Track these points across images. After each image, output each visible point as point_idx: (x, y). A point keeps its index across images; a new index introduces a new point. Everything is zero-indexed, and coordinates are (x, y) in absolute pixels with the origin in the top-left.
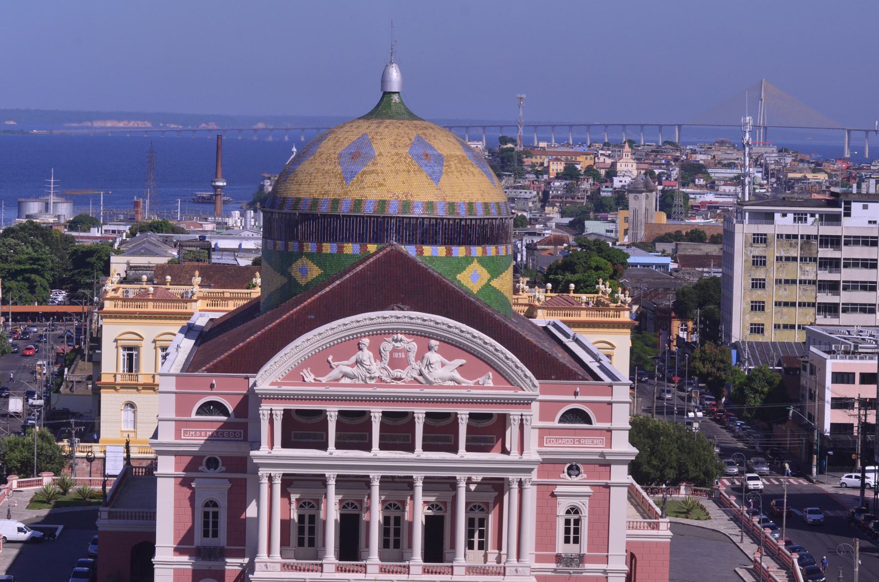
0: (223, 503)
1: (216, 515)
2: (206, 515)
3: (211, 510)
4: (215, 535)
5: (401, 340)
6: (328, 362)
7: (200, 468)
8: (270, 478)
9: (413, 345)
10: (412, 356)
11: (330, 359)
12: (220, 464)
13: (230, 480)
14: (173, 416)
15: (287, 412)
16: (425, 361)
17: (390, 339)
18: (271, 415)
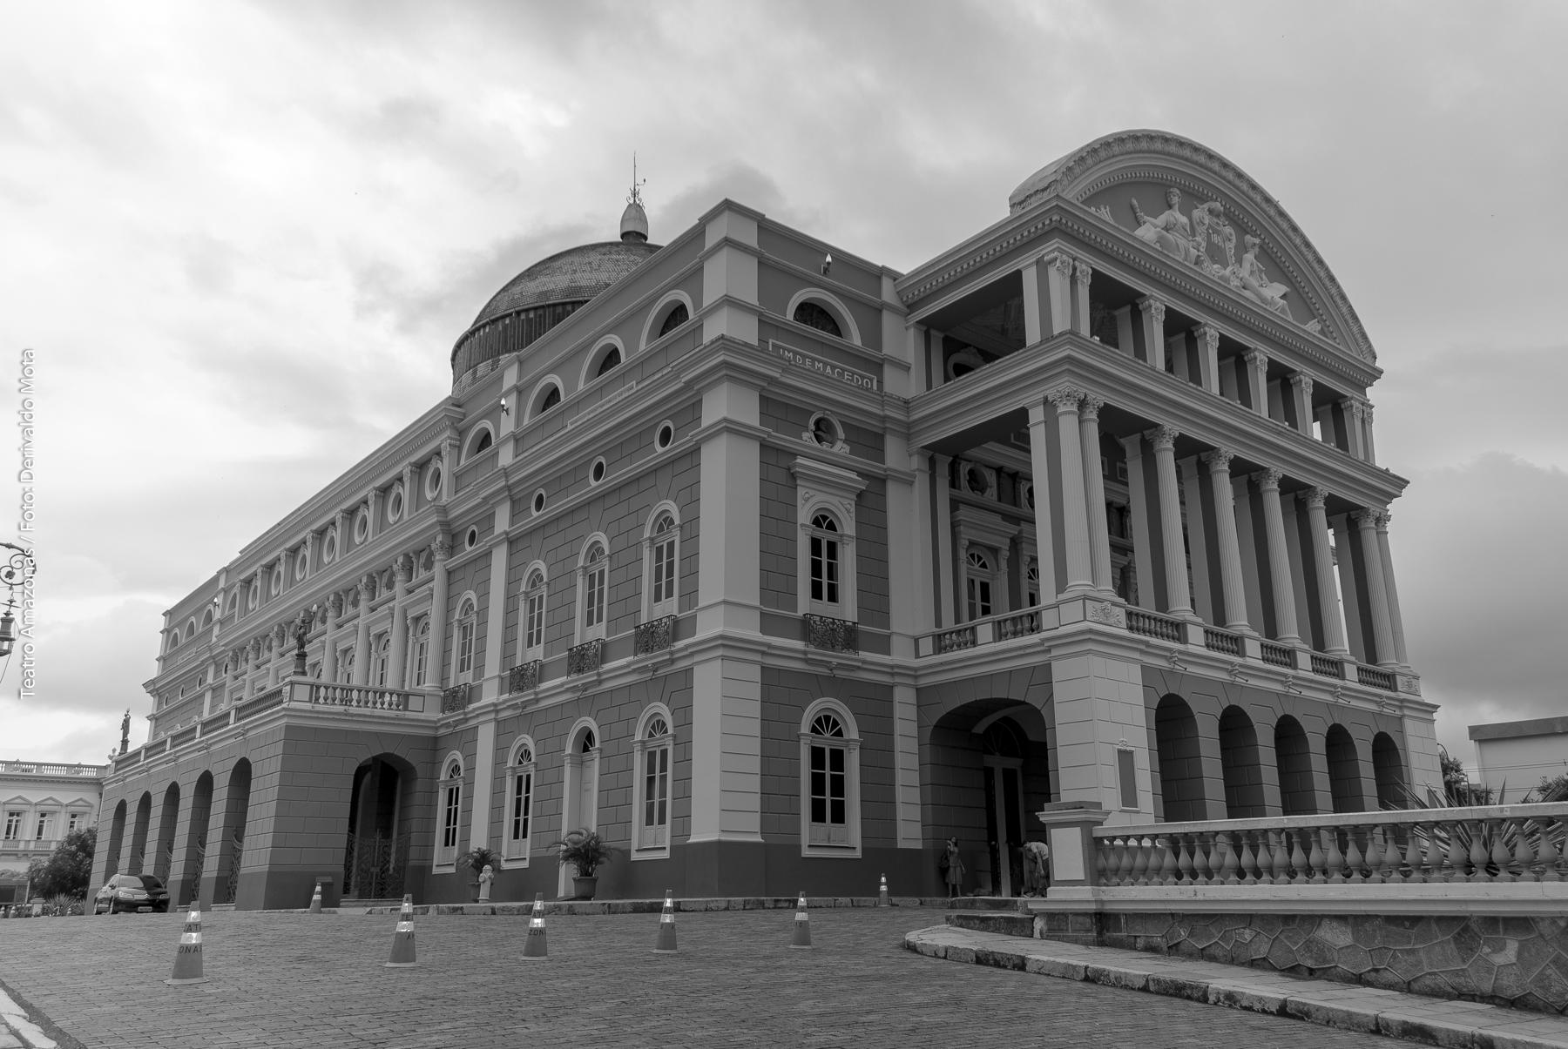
0: (848, 526)
1: (832, 547)
2: (816, 545)
3: (825, 536)
4: (833, 597)
5: (1218, 216)
6: (1132, 207)
7: (806, 435)
8: (1082, 404)
9: (1228, 230)
10: (1230, 247)
11: (1135, 202)
12: (841, 434)
13: (859, 474)
14: (753, 299)
15: (1096, 274)
16: (1246, 265)
17: (1206, 206)
18: (1075, 269)
